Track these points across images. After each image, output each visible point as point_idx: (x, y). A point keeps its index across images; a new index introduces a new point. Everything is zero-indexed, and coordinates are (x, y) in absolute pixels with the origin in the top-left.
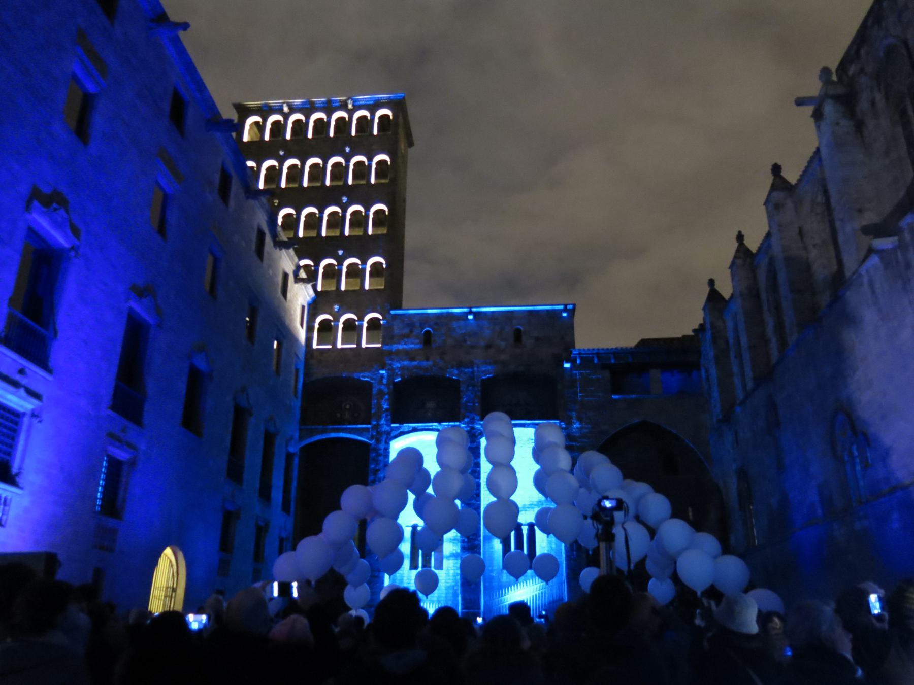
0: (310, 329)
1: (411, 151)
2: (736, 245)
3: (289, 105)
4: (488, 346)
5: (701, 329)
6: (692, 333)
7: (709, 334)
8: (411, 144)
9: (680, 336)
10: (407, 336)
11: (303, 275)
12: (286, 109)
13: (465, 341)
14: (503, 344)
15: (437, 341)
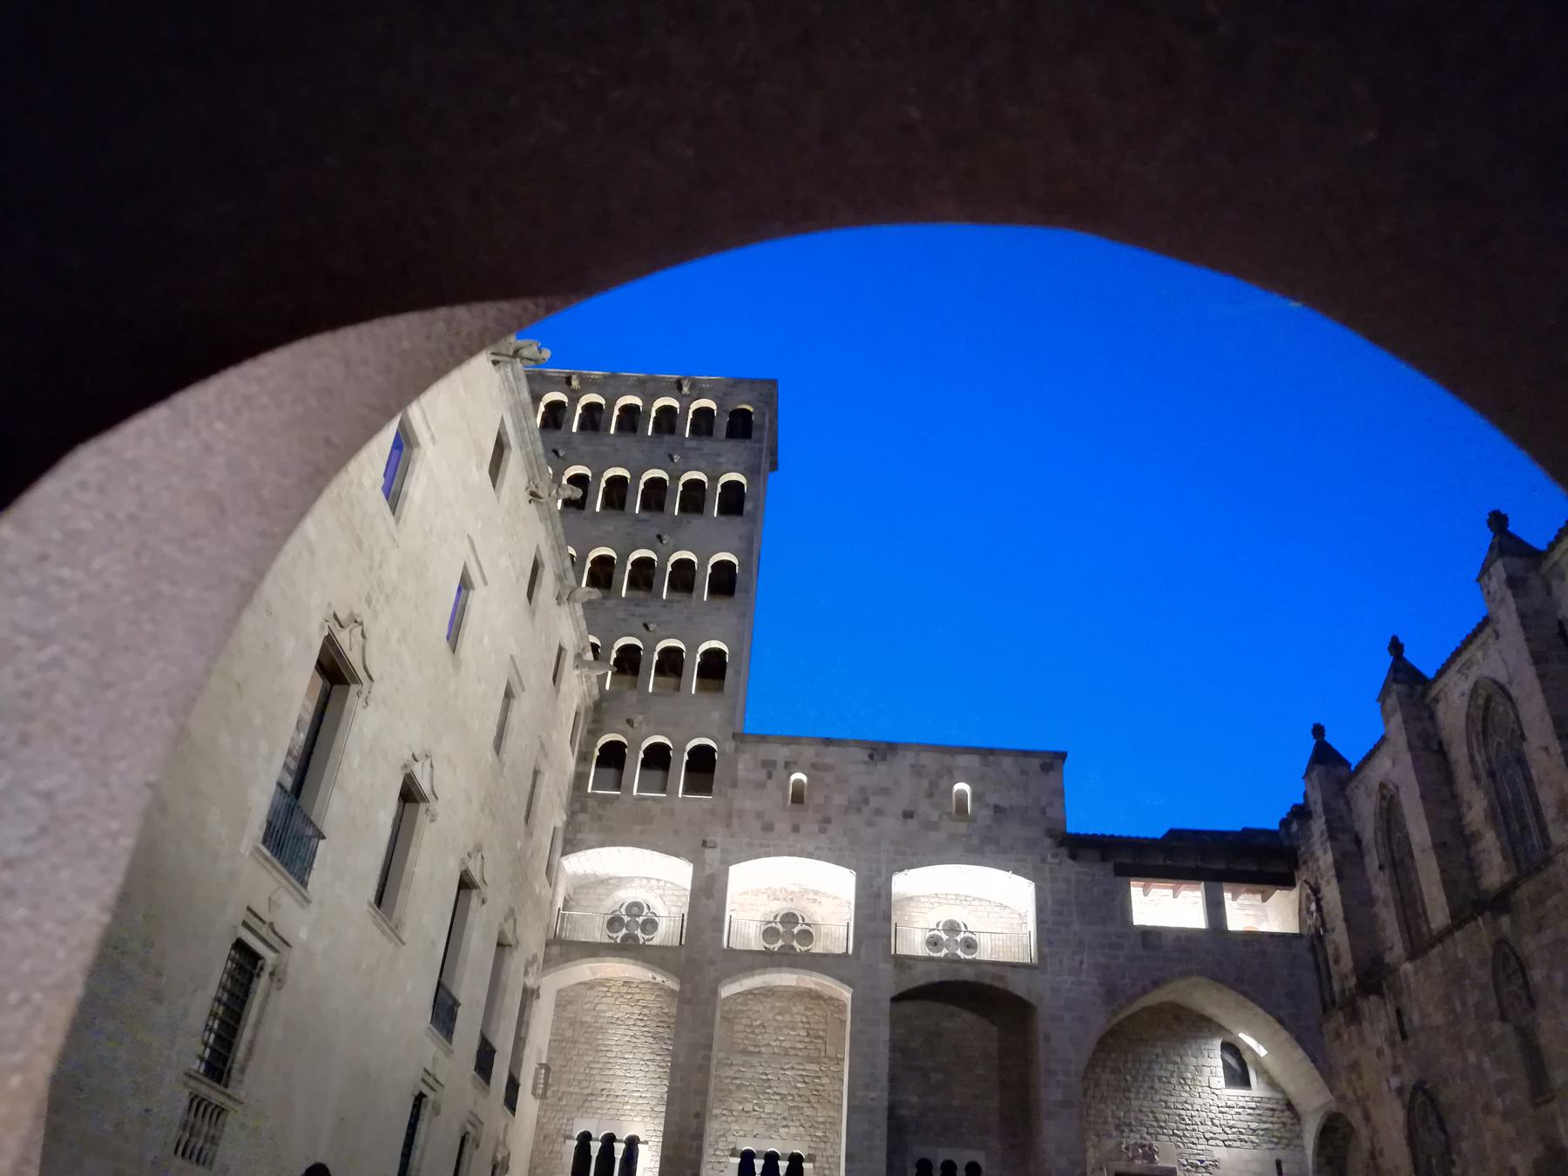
0: (583, 758)
1: (771, 476)
2: (1387, 660)
3: (582, 379)
4: (908, 815)
5: (1301, 813)
6: (1276, 827)
7: (1318, 825)
8: (774, 466)
9: (1239, 829)
10: (760, 785)
11: (589, 656)
12: (575, 383)
13: (866, 801)
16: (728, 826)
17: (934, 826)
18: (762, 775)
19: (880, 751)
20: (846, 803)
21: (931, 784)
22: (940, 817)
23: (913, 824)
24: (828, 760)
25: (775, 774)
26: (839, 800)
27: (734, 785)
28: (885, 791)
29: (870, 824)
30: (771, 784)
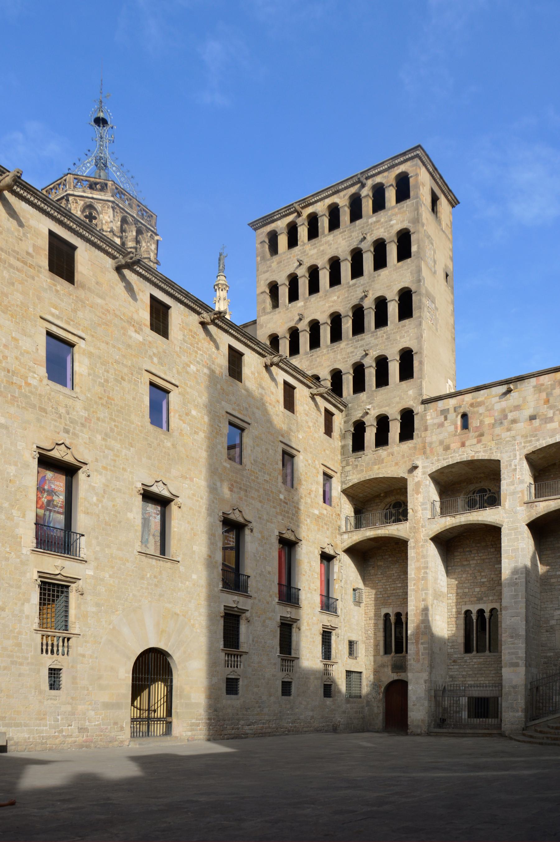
4: (532, 418)
10: (441, 425)
13: (506, 417)
14: (550, 414)
15: (473, 422)
16: (424, 453)
17: (551, 420)
18: (442, 418)
19: (510, 383)
20: (493, 421)
21: (547, 394)
22: (554, 414)
23: (536, 423)
24: (479, 400)
25: (449, 416)
26: (488, 421)
27: (426, 430)
28: (517, 408)
29: (509, 430)
30: (446, 424)
